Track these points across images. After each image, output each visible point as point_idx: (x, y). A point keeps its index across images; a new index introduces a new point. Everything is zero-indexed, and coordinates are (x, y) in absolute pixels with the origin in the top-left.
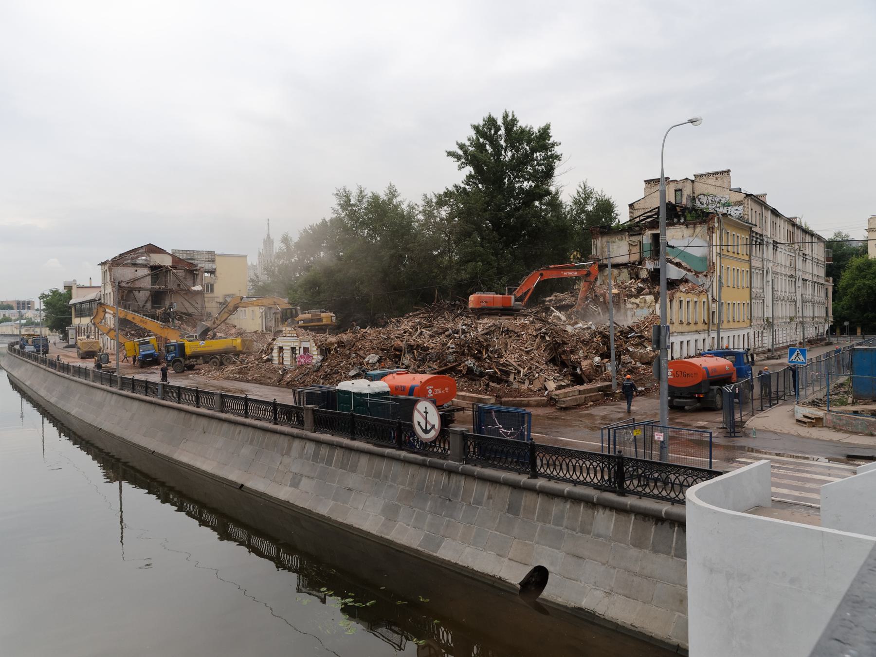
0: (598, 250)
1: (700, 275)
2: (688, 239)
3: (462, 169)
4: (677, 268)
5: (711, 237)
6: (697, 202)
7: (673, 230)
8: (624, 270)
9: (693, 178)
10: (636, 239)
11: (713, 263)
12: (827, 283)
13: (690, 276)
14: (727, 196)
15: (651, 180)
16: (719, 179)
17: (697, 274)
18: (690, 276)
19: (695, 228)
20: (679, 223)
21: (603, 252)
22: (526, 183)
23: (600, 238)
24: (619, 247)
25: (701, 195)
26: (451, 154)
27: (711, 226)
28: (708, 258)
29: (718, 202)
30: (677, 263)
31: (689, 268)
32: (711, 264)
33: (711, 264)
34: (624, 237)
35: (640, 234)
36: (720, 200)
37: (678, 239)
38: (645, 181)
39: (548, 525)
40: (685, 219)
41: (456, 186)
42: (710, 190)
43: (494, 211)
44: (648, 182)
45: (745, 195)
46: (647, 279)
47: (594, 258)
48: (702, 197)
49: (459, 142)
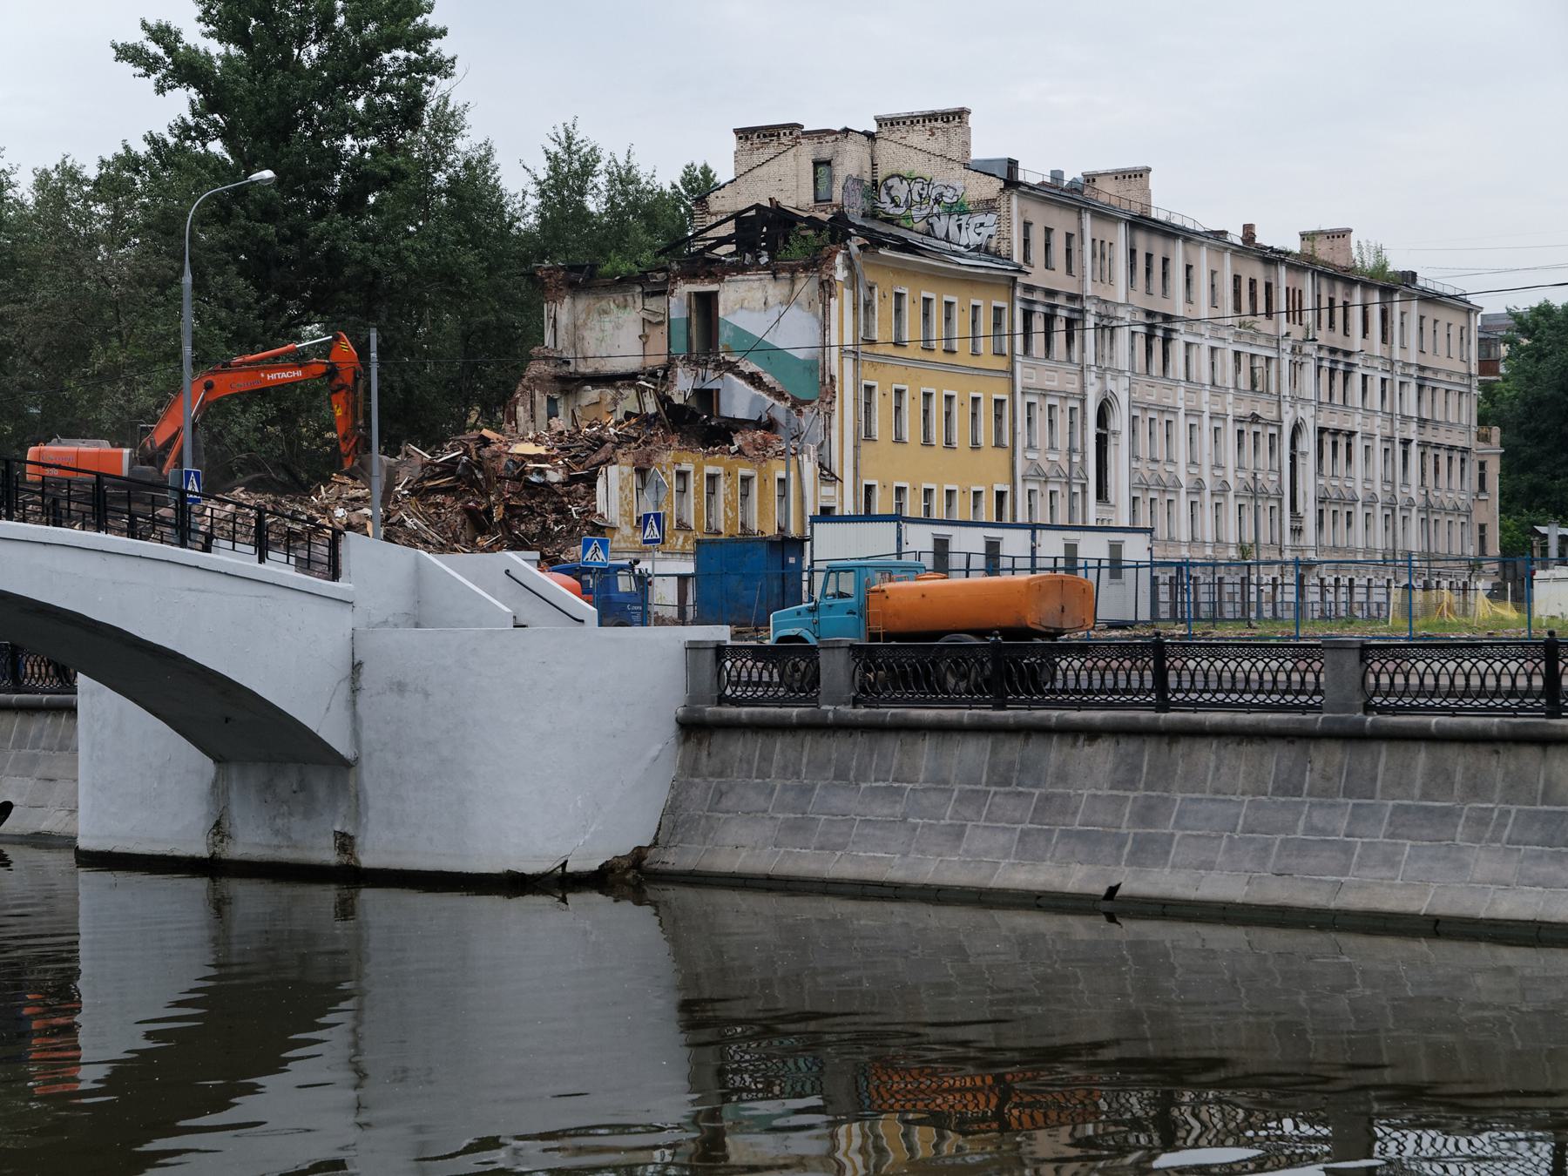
0: (561, 333)
1: (806, 410)
2: (776, 309)
3: (168, 92)
4: (751, 389)
5: (826, 307)
6: (885, 198)
7: (743, 287)
8: (626, 392)
9: (873, 128)
10: (654, 304)
11: (832, 378)
12: (1482, 445)
13: (780, 410)
14: (958, 185)
15: (753, 130)
16: (938, 133)
17: (797, 404)
18: (780, 410)
19: (793, 281)
20: (756, 266)
21: (576, 340)
22: (349, 141)
23: (567, 300)
24: (618, 327)
25: (893, 176)
26: (128, 53)
27: (825, 277)
28: (821, 362)
29: (937, 201)
30: (752, 374)
31: (779, 388)
32: (828, 380)
33: (828, 380)
34: (630, 299)
35: (663, 293)
36: (941, 195)
37: (753, 310)
38: (736, 131)
39: (23, 751)
40: (772, 257)
41: (152, 140)
42: (916, 164)
43: (248, 218)
44: (744, 134)
45: (1002, 185)
46: (655, 415)
47: (546, 358)
48: (895, 182)
49: (152, 22)
